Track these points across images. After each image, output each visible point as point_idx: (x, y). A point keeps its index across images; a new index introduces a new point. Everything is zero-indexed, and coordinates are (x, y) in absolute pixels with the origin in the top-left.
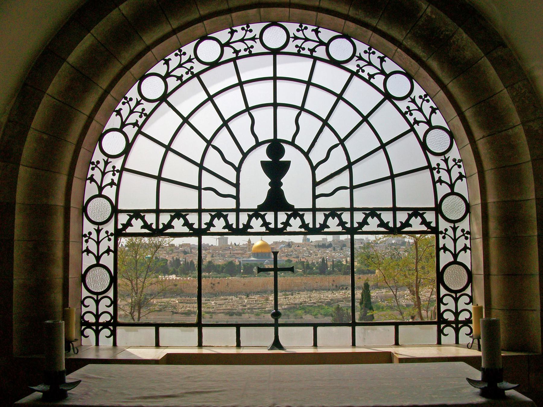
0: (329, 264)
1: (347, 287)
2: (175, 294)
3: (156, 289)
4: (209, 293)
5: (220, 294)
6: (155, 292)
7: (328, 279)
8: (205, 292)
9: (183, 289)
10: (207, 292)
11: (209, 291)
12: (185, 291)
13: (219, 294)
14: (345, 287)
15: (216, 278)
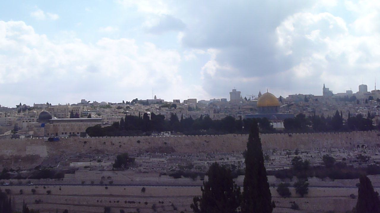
0: (345, 117)
1: (364, 145)
2: (165, 153)
3: (144, 148)
4: (203, 152)
5: (215, 153)
6: (143, 151)
7: (340, 136)
8: (198, 151)
9: (174, 148)
10: (200, 151)
11: (203, 150)
12: (176, 150)
13: (214, 153)
14: (360, 146)
15: (210, 135)
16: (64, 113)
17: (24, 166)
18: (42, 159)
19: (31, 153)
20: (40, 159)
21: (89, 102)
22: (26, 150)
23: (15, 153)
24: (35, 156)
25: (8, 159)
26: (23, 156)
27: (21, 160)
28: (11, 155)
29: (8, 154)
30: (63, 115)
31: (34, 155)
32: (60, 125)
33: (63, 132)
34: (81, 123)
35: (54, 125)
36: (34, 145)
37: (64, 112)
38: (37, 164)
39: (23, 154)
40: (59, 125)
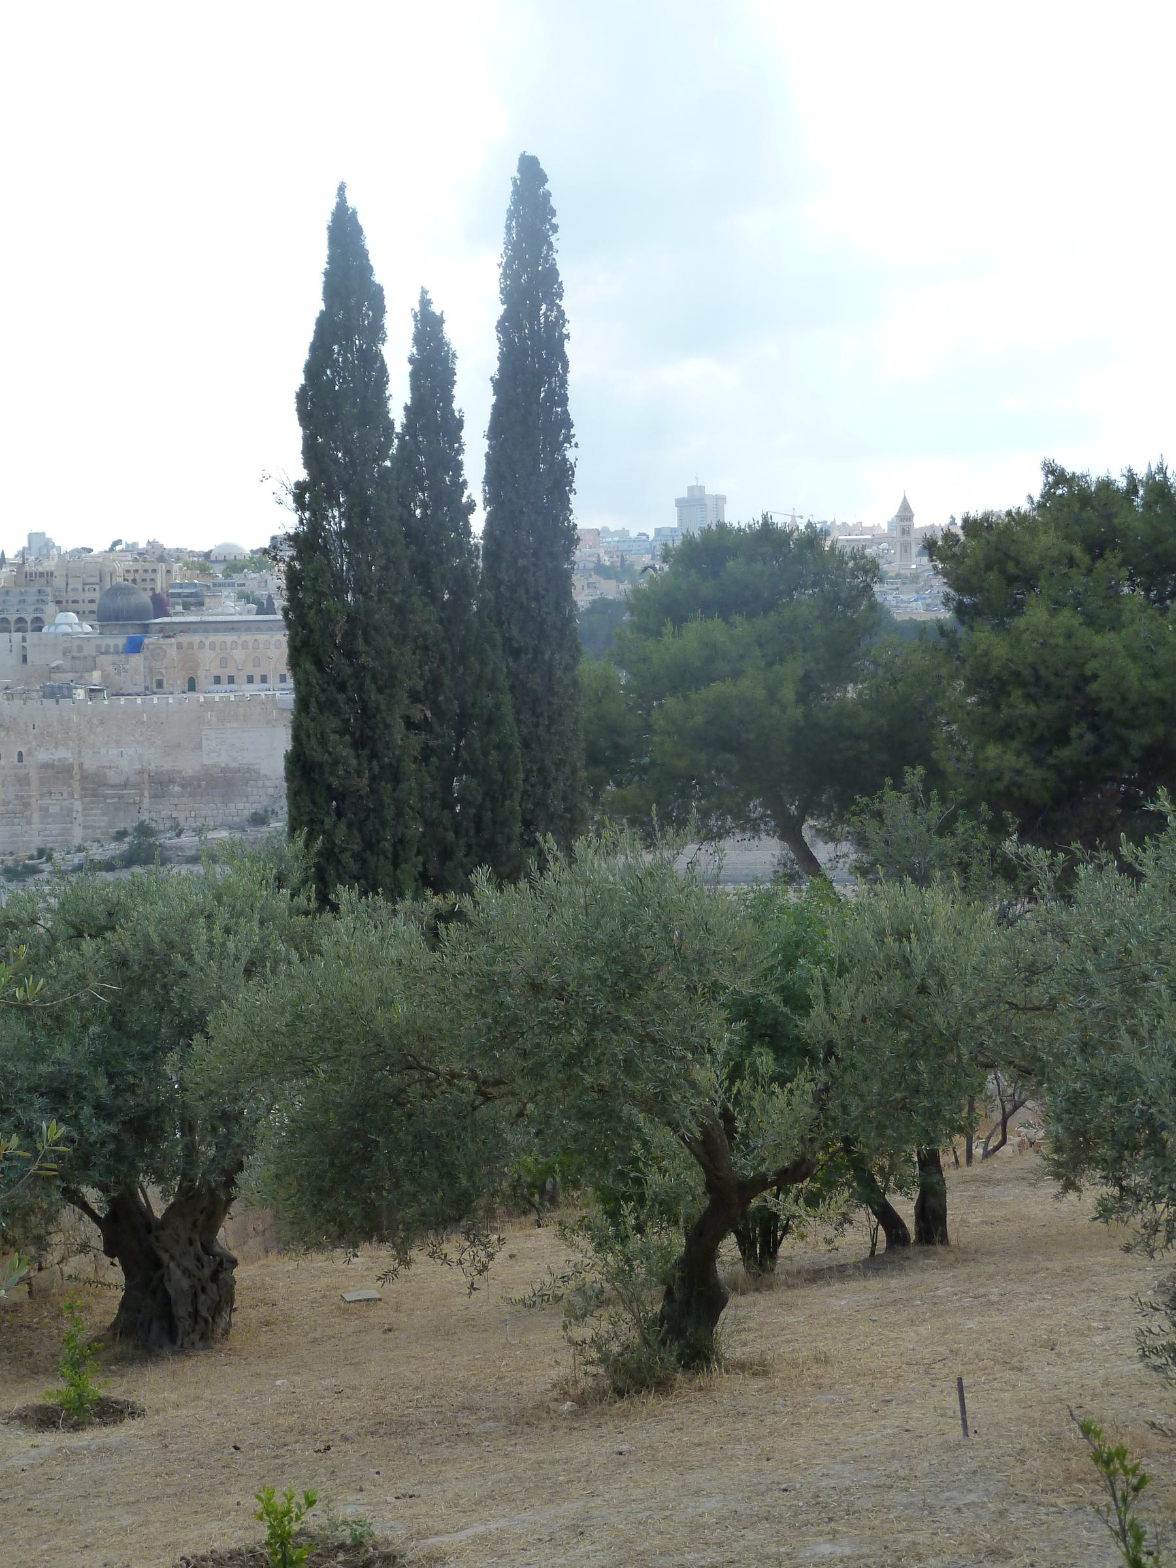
17: (193, 814)
18: (268, 783)
19: (223, 760)
20: (260, 783)
21: (119, 542)
22: (198, 747)
23: (156, 760)
24: (238, 771)
25: (125, 785)
27: (183, 786)
28: (138, 766)
29: (123, 763)
31: (234, 765)
32: (207, 643)
33: (217, 672)
36: (235, 725)
37: (97, 587)
38: (247, 802)
39: (188, 765)
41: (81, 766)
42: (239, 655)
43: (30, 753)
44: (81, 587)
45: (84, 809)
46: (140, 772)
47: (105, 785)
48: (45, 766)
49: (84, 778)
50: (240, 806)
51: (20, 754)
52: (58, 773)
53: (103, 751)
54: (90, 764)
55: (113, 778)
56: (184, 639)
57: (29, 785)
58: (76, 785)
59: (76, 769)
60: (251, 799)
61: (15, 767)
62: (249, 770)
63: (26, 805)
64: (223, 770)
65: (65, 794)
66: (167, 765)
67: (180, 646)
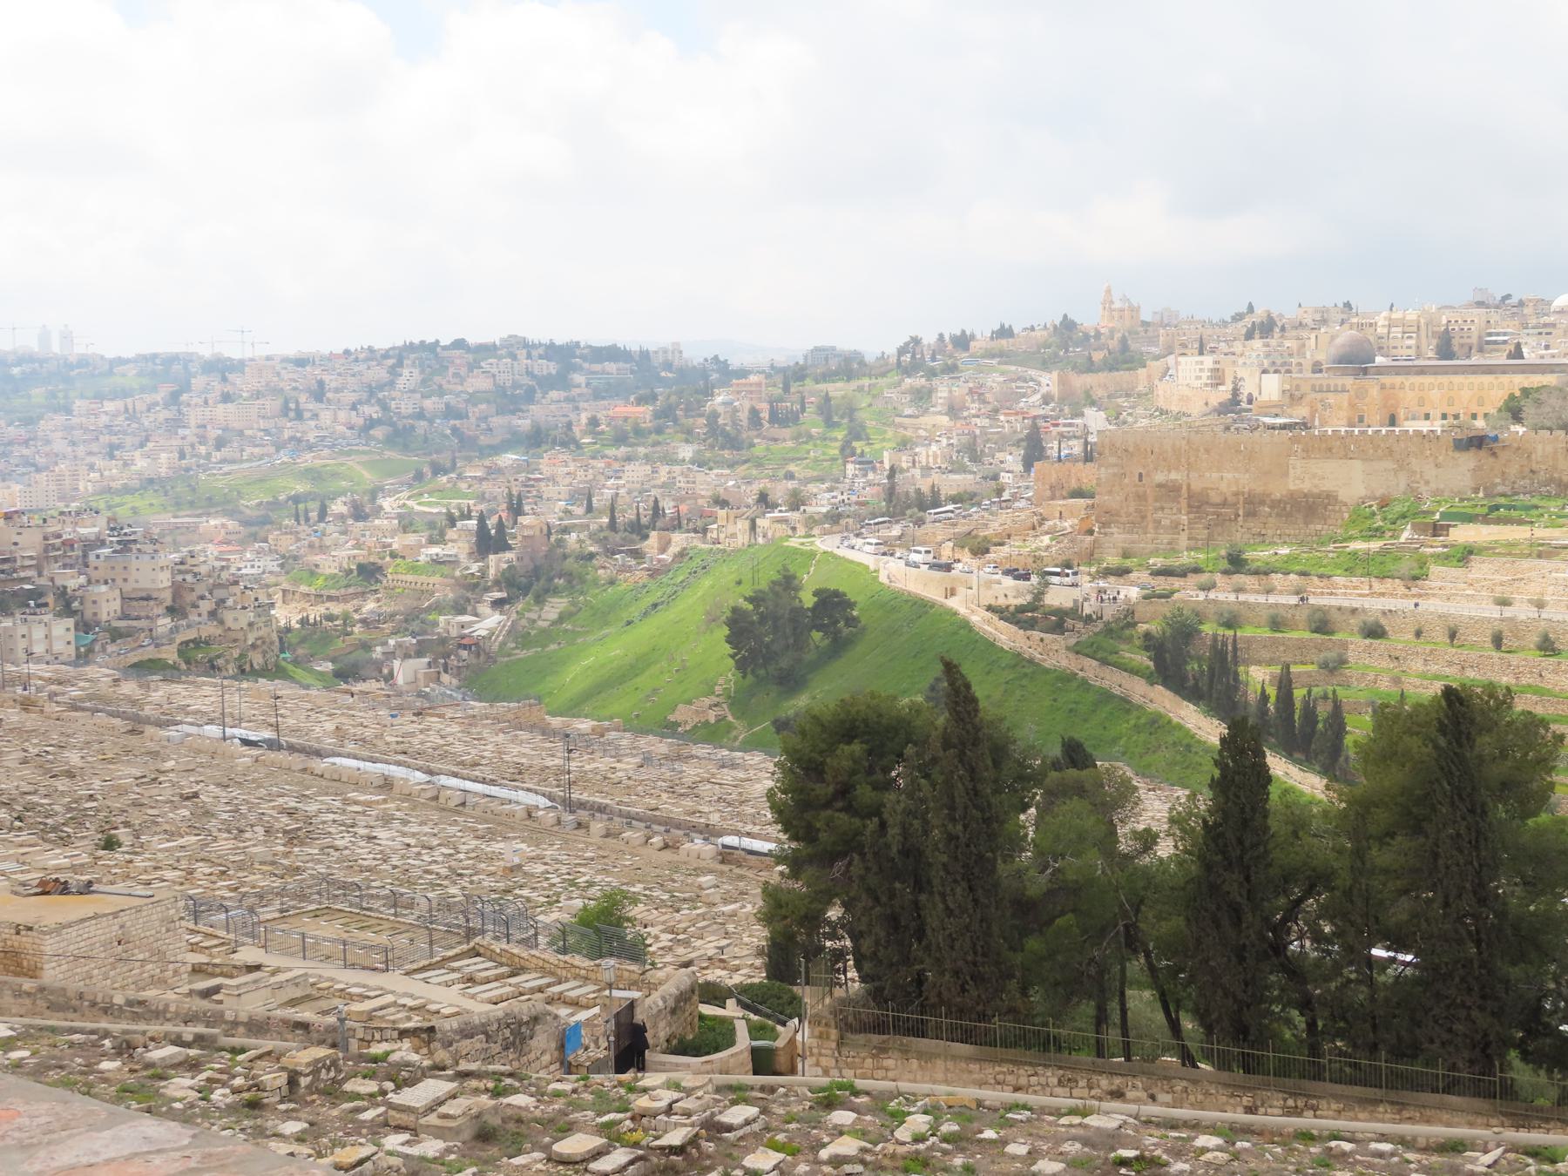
16: (1412, 342)
18: (1344, 508)
19: (1306, 486)
20: (1337, 508)
21: (1508, 296)
22: (1286, 474)
25: (1224, 504)
26: (1277, 496)
27: (1271, 507)
29: (1223, 487)
30: (1409, 347)
31: (1316, 491)
32: (1407, 384)
34: (1487, 379)
35: (1383, 387)
40: (1402, 387)
41: (1189, 486)
42: (1435, 395)
43: (1148, 475)
44: (1400, 335)
45: (1189, 523)
46: (1236, 494)
47: (1207, 503)
48: (1160, 486)
49: (1190, 497)
50: (1319, 527)
51: (1141, 475)
52: (1170, 491)
53: (1208, 475)
54: (1196, 486)
55: (1215, 498)
56: (1387, 380)
57: (1146, 500)
58: (1184, 503)
59: (1185, 488)
60: (1329, 522)
61: (1135, 486)
62: (1328, 496)
63: (1143, 517)
64: (1306, 496)
65: (1175, 510)
66: (1258, 488)
67: (1383, 387)
